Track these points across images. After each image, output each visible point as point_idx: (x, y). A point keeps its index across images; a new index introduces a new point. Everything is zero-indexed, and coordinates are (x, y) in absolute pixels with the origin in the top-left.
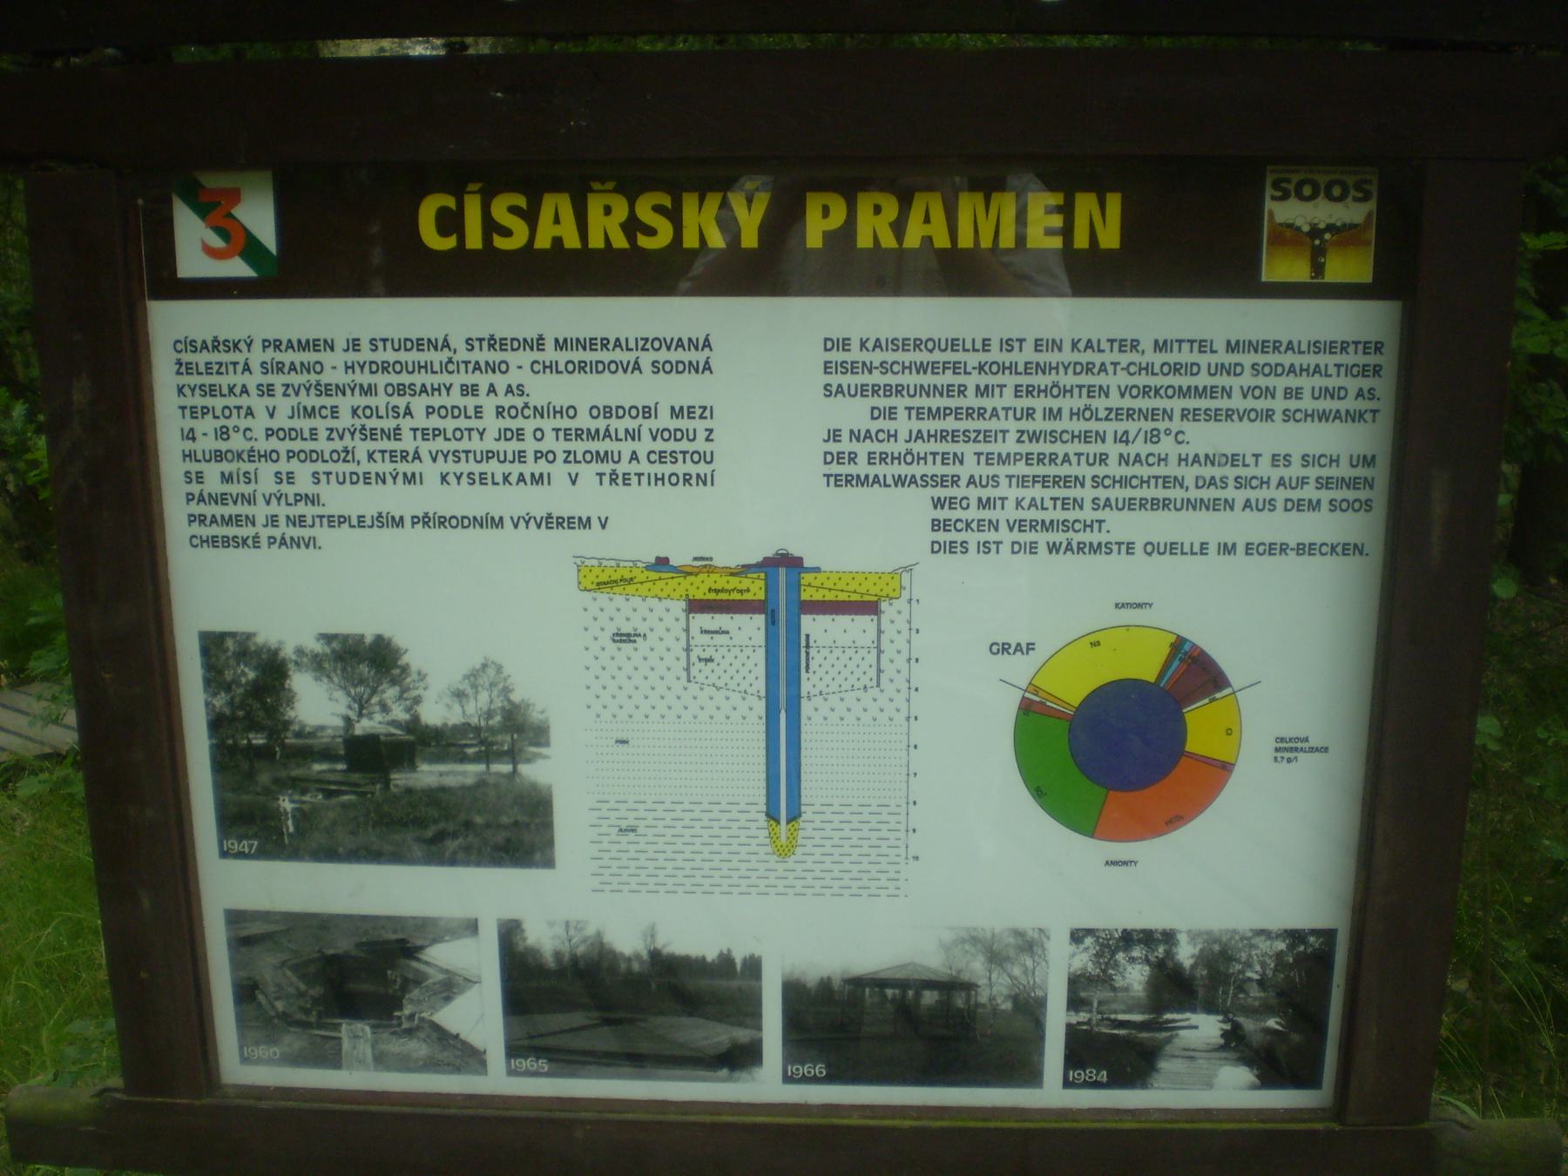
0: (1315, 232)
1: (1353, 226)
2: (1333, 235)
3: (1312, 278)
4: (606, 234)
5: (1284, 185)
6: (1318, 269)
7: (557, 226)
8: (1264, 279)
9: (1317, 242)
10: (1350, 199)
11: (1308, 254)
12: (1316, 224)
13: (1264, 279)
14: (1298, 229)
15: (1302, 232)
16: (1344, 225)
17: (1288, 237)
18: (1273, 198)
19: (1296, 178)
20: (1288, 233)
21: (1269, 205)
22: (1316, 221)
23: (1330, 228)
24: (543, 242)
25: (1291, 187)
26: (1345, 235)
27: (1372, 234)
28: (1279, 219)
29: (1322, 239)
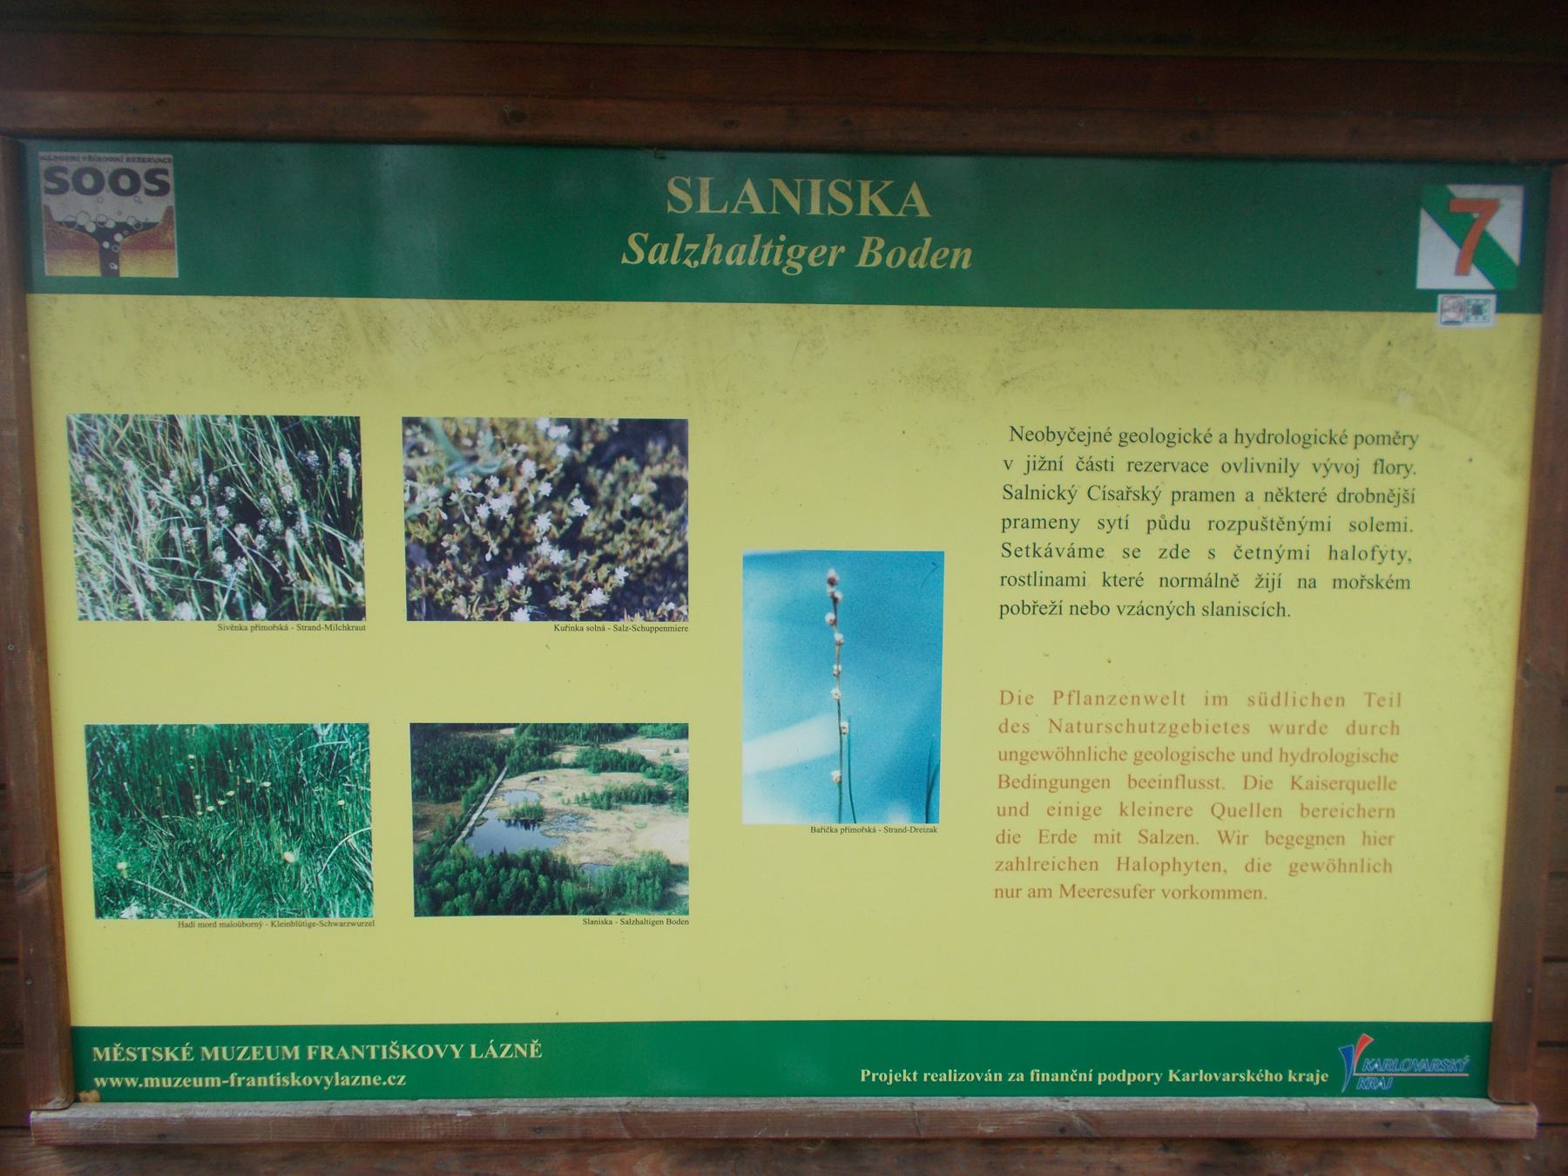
0: (103, 233)
2: (124, 236)
5: (60, 175)
10: (141, 193)
11: (96, 258)
12: (102, 223)
14: (82, 229)
15: (86, 232)
16: (138, 225)
18: (49, 191)
19: (72, 167)
20: (71, 234)
22: (102, 219)
23: (121, 227)
25: (68, 178)
27: (172, 236)
28: (58, 216)
29: (113, 242)
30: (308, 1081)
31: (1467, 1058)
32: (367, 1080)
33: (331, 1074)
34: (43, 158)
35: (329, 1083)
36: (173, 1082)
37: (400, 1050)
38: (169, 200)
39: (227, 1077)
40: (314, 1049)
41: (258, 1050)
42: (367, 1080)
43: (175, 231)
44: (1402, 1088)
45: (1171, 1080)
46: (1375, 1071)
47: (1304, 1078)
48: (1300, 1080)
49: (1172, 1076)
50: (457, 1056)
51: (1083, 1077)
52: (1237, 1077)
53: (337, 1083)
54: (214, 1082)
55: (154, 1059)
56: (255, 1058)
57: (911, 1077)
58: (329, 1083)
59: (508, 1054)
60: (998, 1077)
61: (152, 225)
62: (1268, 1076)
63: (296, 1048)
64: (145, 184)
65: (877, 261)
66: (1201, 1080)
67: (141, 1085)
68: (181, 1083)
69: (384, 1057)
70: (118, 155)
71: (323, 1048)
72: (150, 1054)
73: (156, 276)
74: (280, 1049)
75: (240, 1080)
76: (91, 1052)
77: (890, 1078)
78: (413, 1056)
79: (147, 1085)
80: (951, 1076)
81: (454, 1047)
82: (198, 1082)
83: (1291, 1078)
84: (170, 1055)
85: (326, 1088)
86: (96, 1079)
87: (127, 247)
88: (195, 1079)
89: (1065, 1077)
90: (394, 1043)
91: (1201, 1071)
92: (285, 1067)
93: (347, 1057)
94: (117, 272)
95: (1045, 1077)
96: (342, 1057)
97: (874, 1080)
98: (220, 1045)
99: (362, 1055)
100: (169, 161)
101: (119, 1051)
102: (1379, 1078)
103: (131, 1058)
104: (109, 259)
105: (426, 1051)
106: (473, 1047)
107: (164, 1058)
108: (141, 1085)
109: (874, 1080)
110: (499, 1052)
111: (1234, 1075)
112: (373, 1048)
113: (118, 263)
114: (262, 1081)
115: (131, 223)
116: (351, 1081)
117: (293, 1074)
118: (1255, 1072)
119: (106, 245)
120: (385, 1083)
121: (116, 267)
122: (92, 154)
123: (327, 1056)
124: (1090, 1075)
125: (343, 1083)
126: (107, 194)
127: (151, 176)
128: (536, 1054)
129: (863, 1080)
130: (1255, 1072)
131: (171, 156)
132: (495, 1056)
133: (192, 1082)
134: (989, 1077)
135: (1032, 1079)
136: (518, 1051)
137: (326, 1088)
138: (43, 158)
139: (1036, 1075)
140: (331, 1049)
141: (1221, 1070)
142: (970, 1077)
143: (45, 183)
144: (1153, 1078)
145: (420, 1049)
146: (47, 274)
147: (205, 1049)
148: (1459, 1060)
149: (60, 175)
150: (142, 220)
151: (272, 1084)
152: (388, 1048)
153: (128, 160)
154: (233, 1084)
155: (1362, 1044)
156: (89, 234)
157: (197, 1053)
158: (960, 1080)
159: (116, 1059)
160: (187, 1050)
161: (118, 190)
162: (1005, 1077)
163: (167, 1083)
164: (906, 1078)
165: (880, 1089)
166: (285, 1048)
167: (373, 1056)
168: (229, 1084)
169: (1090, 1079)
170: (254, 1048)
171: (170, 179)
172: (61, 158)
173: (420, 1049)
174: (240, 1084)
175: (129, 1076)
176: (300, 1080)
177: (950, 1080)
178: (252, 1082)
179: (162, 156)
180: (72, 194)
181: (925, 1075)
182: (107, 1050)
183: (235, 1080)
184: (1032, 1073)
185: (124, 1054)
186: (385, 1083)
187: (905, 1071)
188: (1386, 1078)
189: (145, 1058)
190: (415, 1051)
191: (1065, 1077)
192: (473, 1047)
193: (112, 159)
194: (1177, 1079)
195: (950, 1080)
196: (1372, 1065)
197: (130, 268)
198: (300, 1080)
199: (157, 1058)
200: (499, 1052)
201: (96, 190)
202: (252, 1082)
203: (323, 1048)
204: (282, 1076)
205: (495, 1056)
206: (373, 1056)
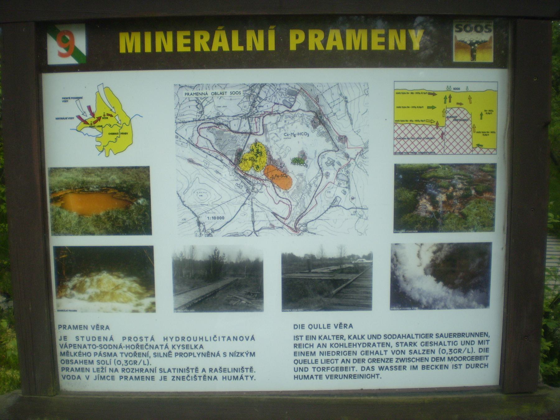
0: (472, 44)
1: (485, 42)
2: (478, 45)
3: (471, 60)
4: (201, 45)
5: (460, 27)
6: (473, 57)
7: (220, 43)
8: (454, 60)
9: (473, 47)
12: (472, 41)
13: (454, 60)
14: (466, 43)
16: (482, 41)
17: (462, 46)
18: (456, 31)
21: (455, 34)
23: (477, 42)
24: (215, 48)
25: (462, 27)
26: (483, 44)
27: (492, 45)
29: (475, 47)
121: (475, 54)
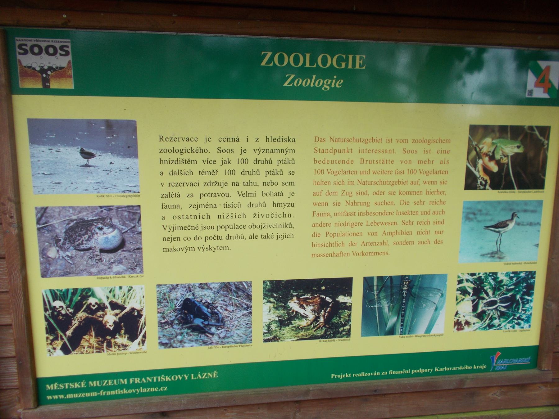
0: (43, 71)
1: (62, 68)
2: (52, 72)
10: (58, 55)
11: (41, 80)
14: (34, 69)
16: (57, 68)
18: (20, 54)
19: (30, 44)
20: (30, 71)
22: (42, 65)
23: (50, 68)
27: (71, 72)
28: (24, 64)
29: (47, 74)
30: (130, 391)
31: (530, 358)
32: (153, 389)
33: (139, 388)
34: (17, 40)
35: (138, 391)
36: (78, 395)
37: (165, 378)
38: (69, 58)
39: (99, 392)
40: (132, 380)
41: (111, 381)
42: (153, 389)
43: (72, 70)
44: (509, 368)
45: (436, 371)
46: (501, 364)
47: (479, 367)
48: (477, 368)
49: (436, 369)
50: (186, 378)
51: (407, 372)
52: (457, 368)
53: (141, 391)
54: (94, 394)
55: (70, 387)
56: (110, 384)
57: (349, 376)
58: (138, 391)
59: (206, 376)
60: (378, 373)
61: (63, 68)
62: (467, 367)
63: (126, 380)
64: (59, 51)
65: (325, 81)
66: (445, 370)
67: (65, 398)
68: (81, 395)
69: (159, 380)
70: (48, 40)
71: (136, 379)
72: (69, 386)
73: (68, 88)
74: (120, 381)
75: (104, 393)
76: (46, 387)
77: (341, 376)
78: (170, 380)
79: (68, 397)
80: (363, 374)
81: (185, 375)
82: (88, 395)
83: (475, 367)
84: (77, 385)
85: (137, 393)
86: (48, 397)
87: (52, 76)
88: (87, 394)
89: (401, 372)
90: (163, 376)
91: (446, 367)
92: (122, 387)
93: (145, 382)
94: (49, 86)
95: (394, 373)
96: (143, 382)
97: (336, 377)
98: (97, 380)
99: (151, 380)
100: (69, 42)
101: (57, 385)
102: (502, 366)
103: (62, 388)
104: (45, 81)
105: (175, 378)
106: (192, 375)
107: (75, 387)
108: (65, 398)
109: (336, 377)
110: (202, 376)
111: (456, 368)
112: (155, 378)
113: (49, 83)
114: (113, 393)
115: (54, 67)
116: (147, 390)
117: (125, 389)
118: (463, 366)
119: (44, 75)
120: (159, 390)
121: (48, 84)
122: (37, 39)
123: (137, 382)
124: (409, 371)
125: (144, 391)
126: (44, 55)
127: (62, 48)
128: (216, 376)
129: (332, 377)
130: (463, 366)
131: (69, 40)
132: (200, 377)
133: (86, 395)
134: (375, 374)
135: (390, 374)
136: (209, 376)
137: (137, 393)
138: (17, 40)
139: (391, 372)
140: (139, 379)
141: (452, 367)
142: (369, 374)
143: (18, 50)
144: (430, 371)
145: (173, 378)
146: (20, 87)
147: (90, 382)
148: (527, 358)
149: (24, 47)
150: (59, 66)
151: (117, 393)
152: (160, 378)
153: (52, 41)
154: (101, 395)
155: (498, 355)
156: (37, 71)
157: (87, 384)
158: (365, 375)
159: (55, 388)
160: (84, 383)
161: (48, 53)
162: (381, 374)
163: (76, 396)
164: (347, 376)
165: (338, 380)
166: (121, 380)
167: (155, 381)
168: (100, 394)
169: (409, 372)
170: (110, 381)
171: (69, 50)
172: (25, 40)
173: (173, 378)
174: (104, 394)
175: (61, 394)
176: (127, 391)
177: (362, 375)
178: (109, 393)
179: (66, 40)
180: (30, 55)
181: (354, 375)
182: (52, 385)
183: (102, 393)
184: (390, 371)
185: (59, 386)
186: (159, 390)
187: (346, 374)
188: (505, 366)
189: (67, 387)
190: (171, 378)
191: (401, 372)
192: (192, 375)
193: (45, 41)
194: (438, 370)
195: (362, 375)
196: (500, 361)
197: (54, 85)
198: (127, 391)
199: (72, 387)
200: (202, 376)
201: (40, 53)
202: (109, 393)
203: (136, 379)
204: (120, 390)
205: (200, 377)
206: (155, 381)
